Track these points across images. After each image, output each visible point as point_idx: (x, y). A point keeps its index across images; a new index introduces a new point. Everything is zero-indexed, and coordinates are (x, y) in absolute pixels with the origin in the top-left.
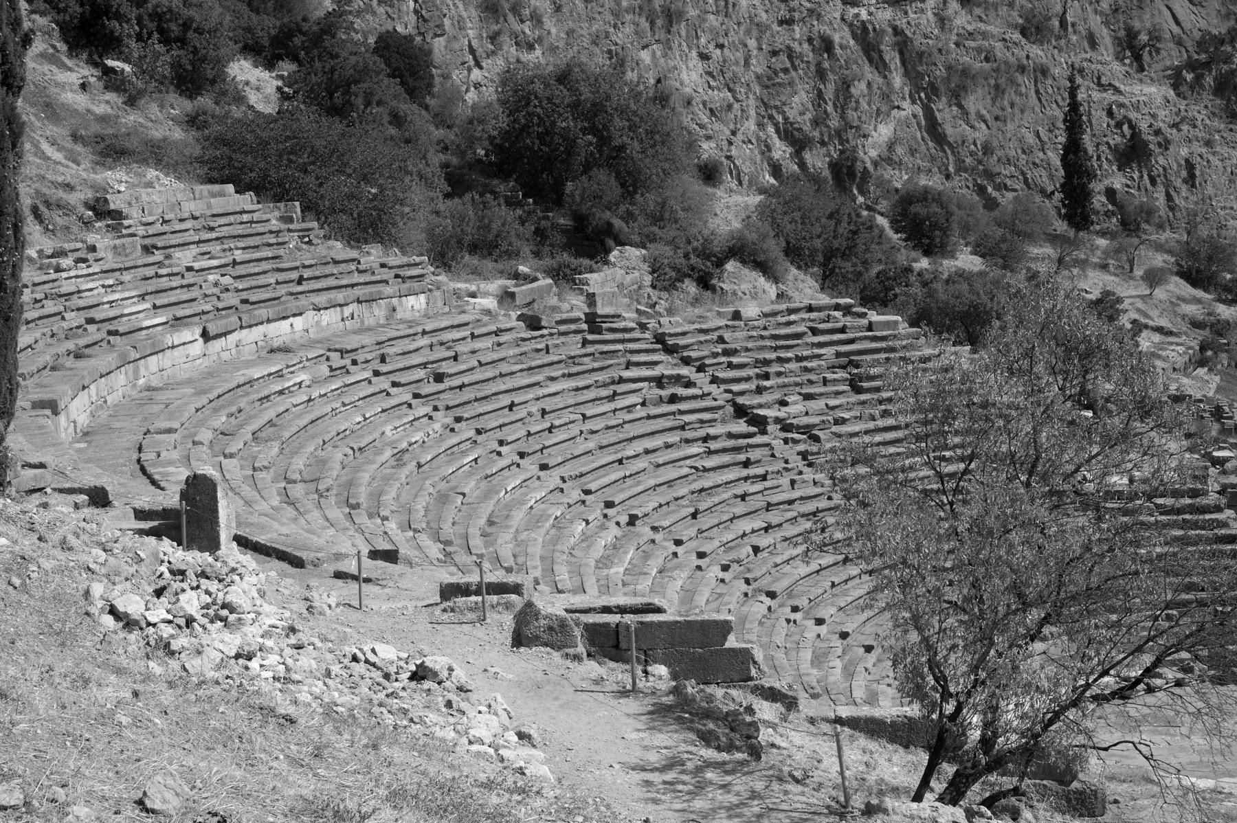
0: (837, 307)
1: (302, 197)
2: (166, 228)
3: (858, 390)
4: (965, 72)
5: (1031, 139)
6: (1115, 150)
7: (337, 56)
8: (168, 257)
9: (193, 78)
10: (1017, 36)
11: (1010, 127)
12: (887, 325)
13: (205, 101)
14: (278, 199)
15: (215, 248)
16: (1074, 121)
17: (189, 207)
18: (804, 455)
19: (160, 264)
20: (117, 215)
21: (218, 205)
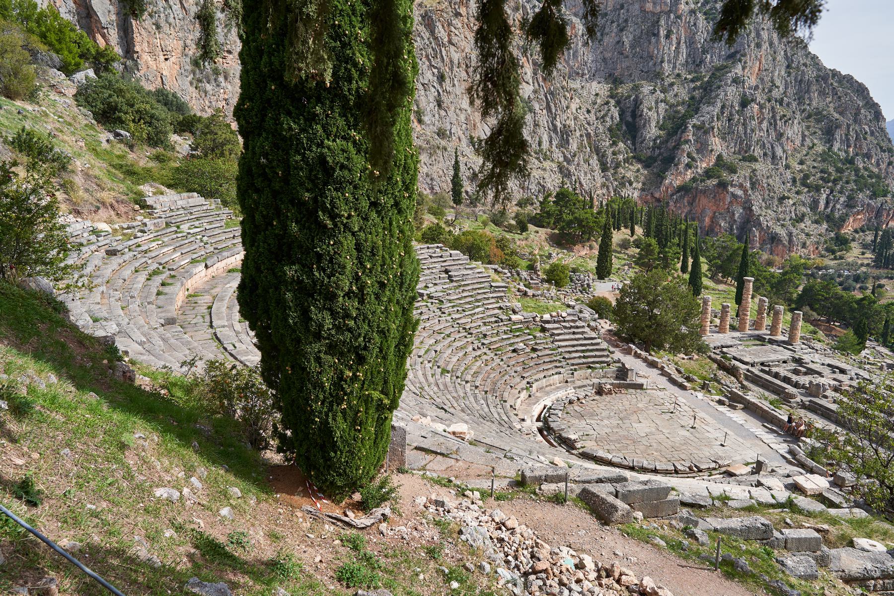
0: (438, 247)
1: (221, 196)
2: (172, 214)
3: (452, 281)
4: (420, 147)
5: (441, 172)
6: (468, 178)
7: (216, 134)
8: (178, 227)
9: (155, 140)
10: (436, 137)
11: (435, 168)
12: (457, 254)
13: (160, 150)
14: (212, 197)
15: (197, 223)
16: (456, 167)
17: (180, 203)
18: (440, 309)
19: (176, 232)
20: (151, 207)
21: (192, 202)
